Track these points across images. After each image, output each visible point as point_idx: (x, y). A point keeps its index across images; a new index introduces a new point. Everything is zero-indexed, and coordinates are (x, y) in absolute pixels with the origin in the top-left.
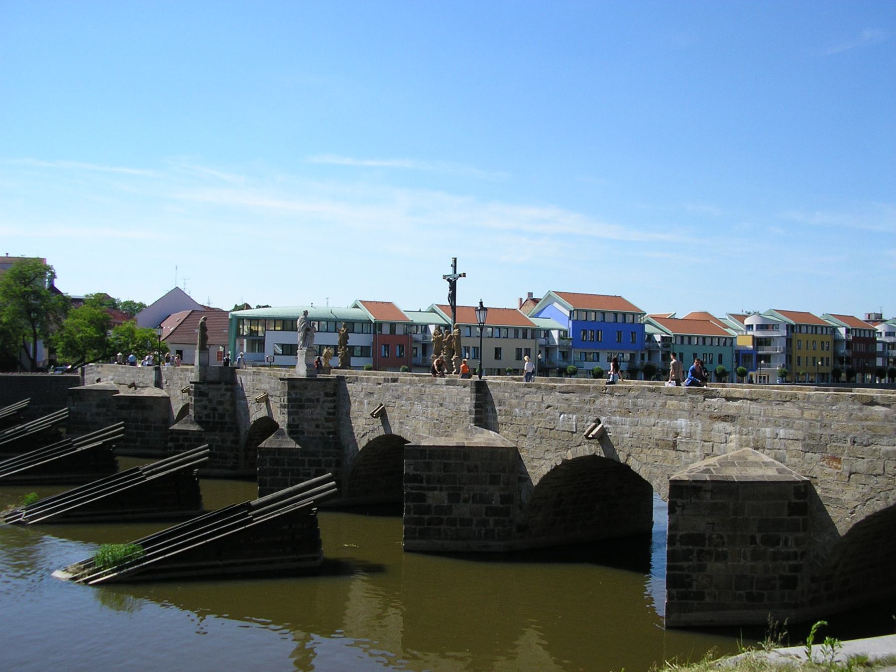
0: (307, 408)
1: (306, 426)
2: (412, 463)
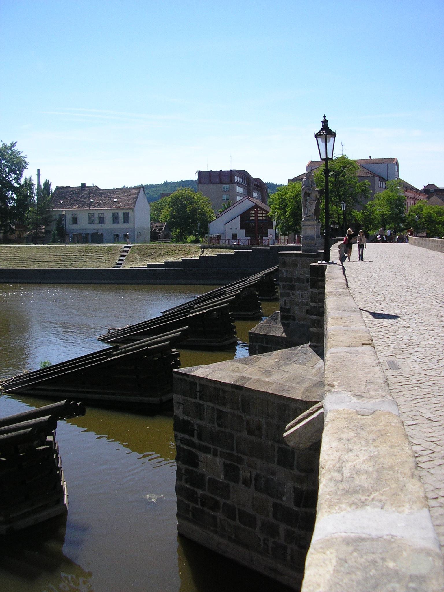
0: (298, 291)
1: (297, 312)
2: (181, 401)
